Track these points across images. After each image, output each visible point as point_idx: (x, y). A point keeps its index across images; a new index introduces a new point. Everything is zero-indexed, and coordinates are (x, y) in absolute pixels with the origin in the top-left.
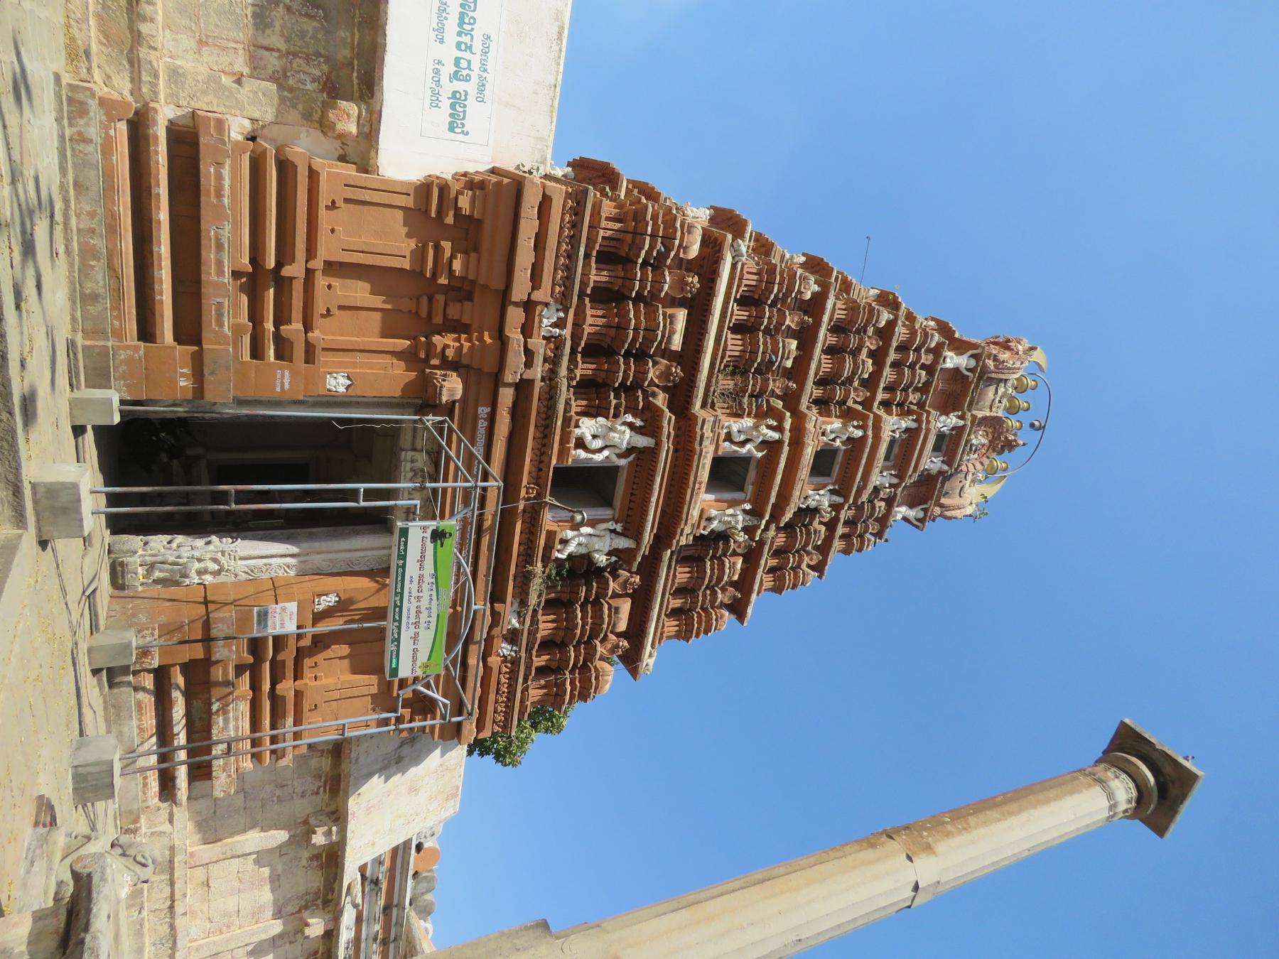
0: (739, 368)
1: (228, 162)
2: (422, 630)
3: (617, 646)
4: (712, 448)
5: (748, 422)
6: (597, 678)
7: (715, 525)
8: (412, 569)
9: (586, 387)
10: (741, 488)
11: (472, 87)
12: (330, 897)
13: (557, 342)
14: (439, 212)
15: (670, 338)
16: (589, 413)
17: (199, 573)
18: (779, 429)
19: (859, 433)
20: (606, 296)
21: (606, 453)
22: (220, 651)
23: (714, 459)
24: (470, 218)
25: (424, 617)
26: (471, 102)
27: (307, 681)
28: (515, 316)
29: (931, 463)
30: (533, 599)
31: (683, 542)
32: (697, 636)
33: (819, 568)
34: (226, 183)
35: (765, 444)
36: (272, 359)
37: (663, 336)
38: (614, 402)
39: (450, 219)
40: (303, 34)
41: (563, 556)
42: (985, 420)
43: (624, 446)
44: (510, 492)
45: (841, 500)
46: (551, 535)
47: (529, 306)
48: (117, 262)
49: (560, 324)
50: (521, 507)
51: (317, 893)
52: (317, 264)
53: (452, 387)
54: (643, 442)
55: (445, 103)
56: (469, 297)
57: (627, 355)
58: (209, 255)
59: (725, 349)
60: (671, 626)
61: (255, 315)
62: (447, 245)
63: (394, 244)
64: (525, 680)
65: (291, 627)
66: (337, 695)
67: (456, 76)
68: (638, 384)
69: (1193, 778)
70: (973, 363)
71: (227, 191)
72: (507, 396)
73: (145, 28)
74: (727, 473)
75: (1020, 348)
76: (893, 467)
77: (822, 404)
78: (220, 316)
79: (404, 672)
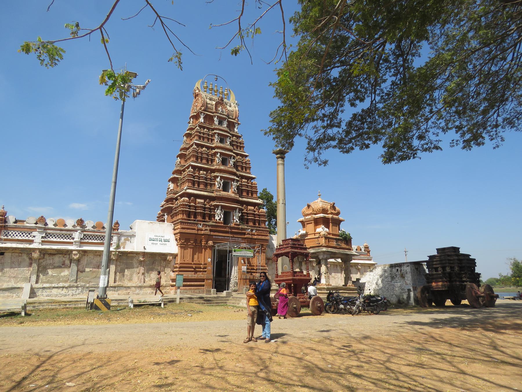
0: (206, 185)
5: (216, 183)
8: (239, 254)
9: (210, 219)
11: (163, 238)
16: (214, 217)
22: (248, 277)
24: (185, 240)
27: (255, 265)
28: (200, 232)
30: (246, 227)
31: (238, 197)
33: (246, 156)
35: (221, 180)
44: (227, 232)
46: (235, 224)
47: (198, 230)
49: (200, 224)
52: (193, 263)
53: (210, 243)
60: (254, 195)
61: (201, 271)
63: (189, 251)
65: (246, 267)
68: (210, 209)
70: (203, 114)
74: (225, 188)
75: (197, 91)
77: (212, 161)
79: (252, 255)
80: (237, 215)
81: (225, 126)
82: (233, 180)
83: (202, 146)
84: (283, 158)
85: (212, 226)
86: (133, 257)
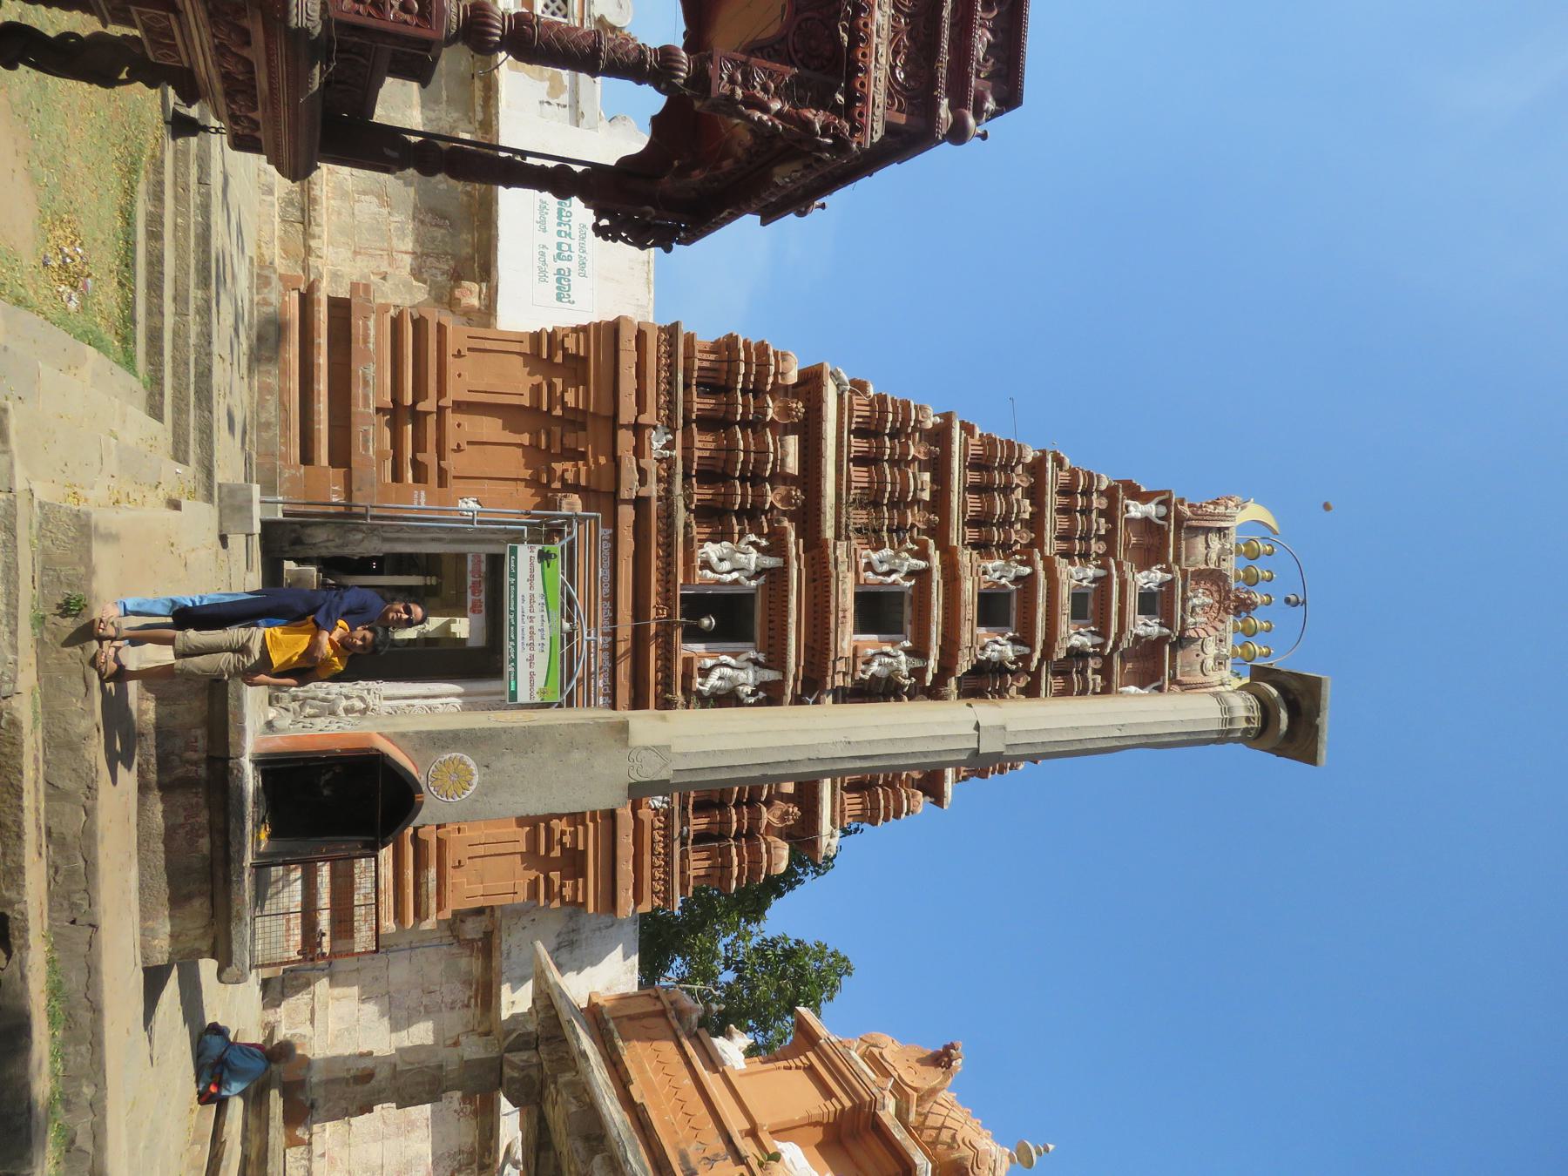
0: (871, 500)
1: (373, 317)
2: (536, 652)
3: (787, 813)
4: (851, 575)
5: (887, 552)
6: (768, 851)
7: (875, 667)
10: (900, 631)
11: (573, 265)
12: (487, 1161)
13: (670, 462)
14: (549, 355)
15: (783, 460)
17: (347, 711)
18: (922, 554)
19: (1028, 570)
20: (712, 423)
21: (735, 575)
23: (858, 597)
25: (537, 637)
26: (574, 277)
28: (626, 439)
29: (1148, 627)
32: (886, 819)
34: (371, 335)
35: (911, 574)
36: (410, 480)
37: (775, 459)
38: (737, 528)
39: (559, 359)
40: (433, 239)
41: (706, 688)
42: (1200, 576)
43: (753, 567)
45: (1027, 650)
46: (688, 662)
47: (638, 429)
48: (286, 398)
49: (670, 446)
50: (652, 632)
51: (471, 1153)
52: (444, 402)
54: (770, 562)
55: (552, 278)
56: (583, 427)
57: (743, 479)
58: (358, 391)
59: (849, 481)
62: (558, 382)
64: (683, 844)
66: (481, 850)
67: (559, 257)
69: (1317, 683)
70: (1163, 510)
71: (372, 340)
72: (627, 514)
73: (313, 243)
76: (1094, 624)
77: (982, 547)
78: (366, 441)
80: (742, 676)
81: (1141, 631)
82: (919, 652)
83: (1035, 494)
84: (1261, 735)
85: (668, 516)
86: (468, 108)
